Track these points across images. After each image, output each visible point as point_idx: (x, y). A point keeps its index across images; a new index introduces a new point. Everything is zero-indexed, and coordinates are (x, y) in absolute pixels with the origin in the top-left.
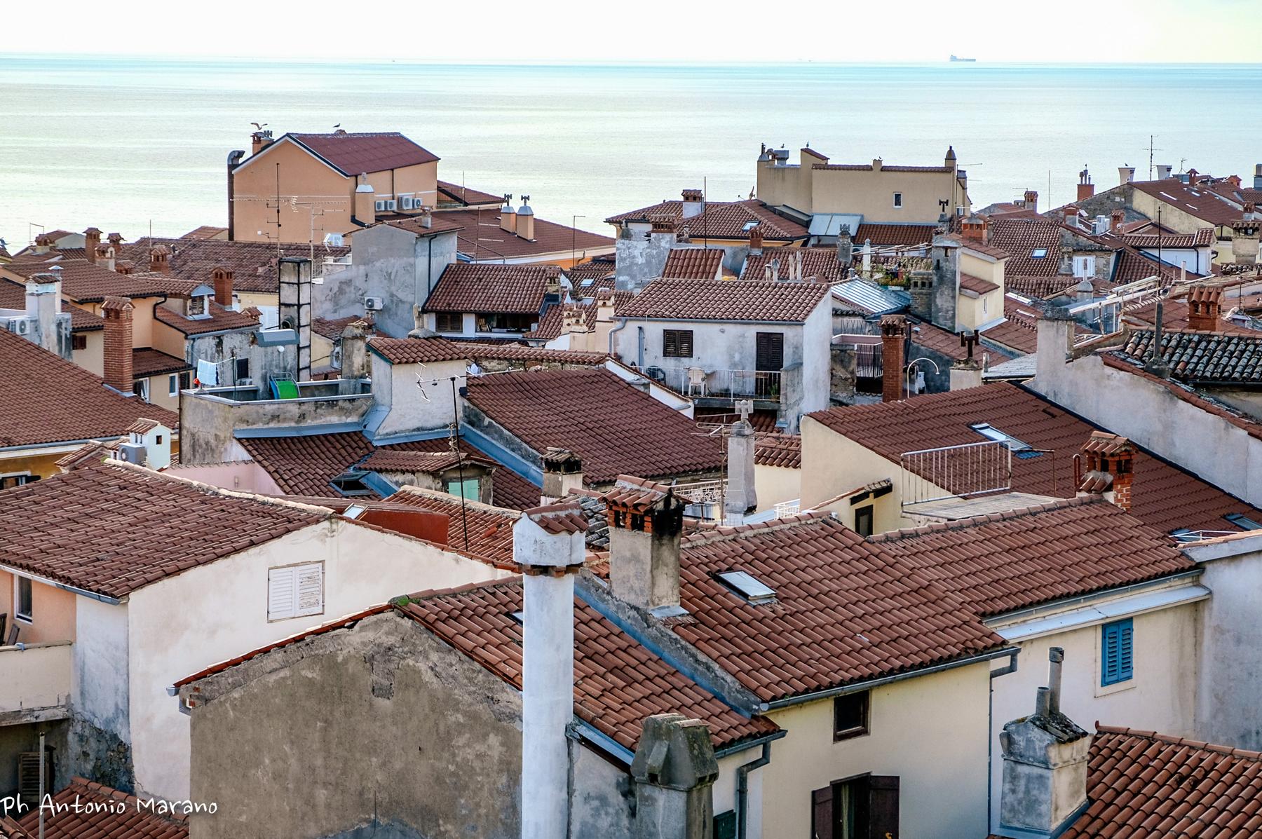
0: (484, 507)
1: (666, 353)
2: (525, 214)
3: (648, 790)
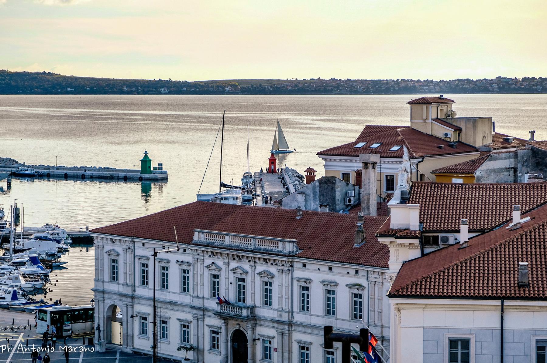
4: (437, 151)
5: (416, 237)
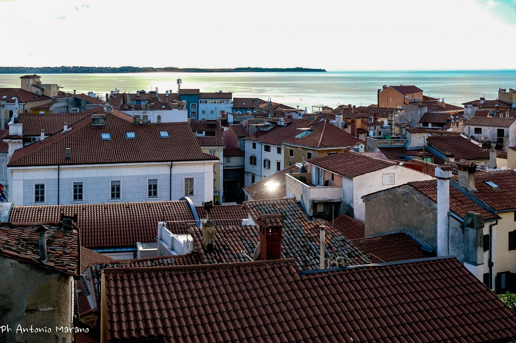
0: (432, 164)
1: (475, 133)
2: (443, 103)
3: (467, 228)
4: (33, 99)
5: (21, 139)
